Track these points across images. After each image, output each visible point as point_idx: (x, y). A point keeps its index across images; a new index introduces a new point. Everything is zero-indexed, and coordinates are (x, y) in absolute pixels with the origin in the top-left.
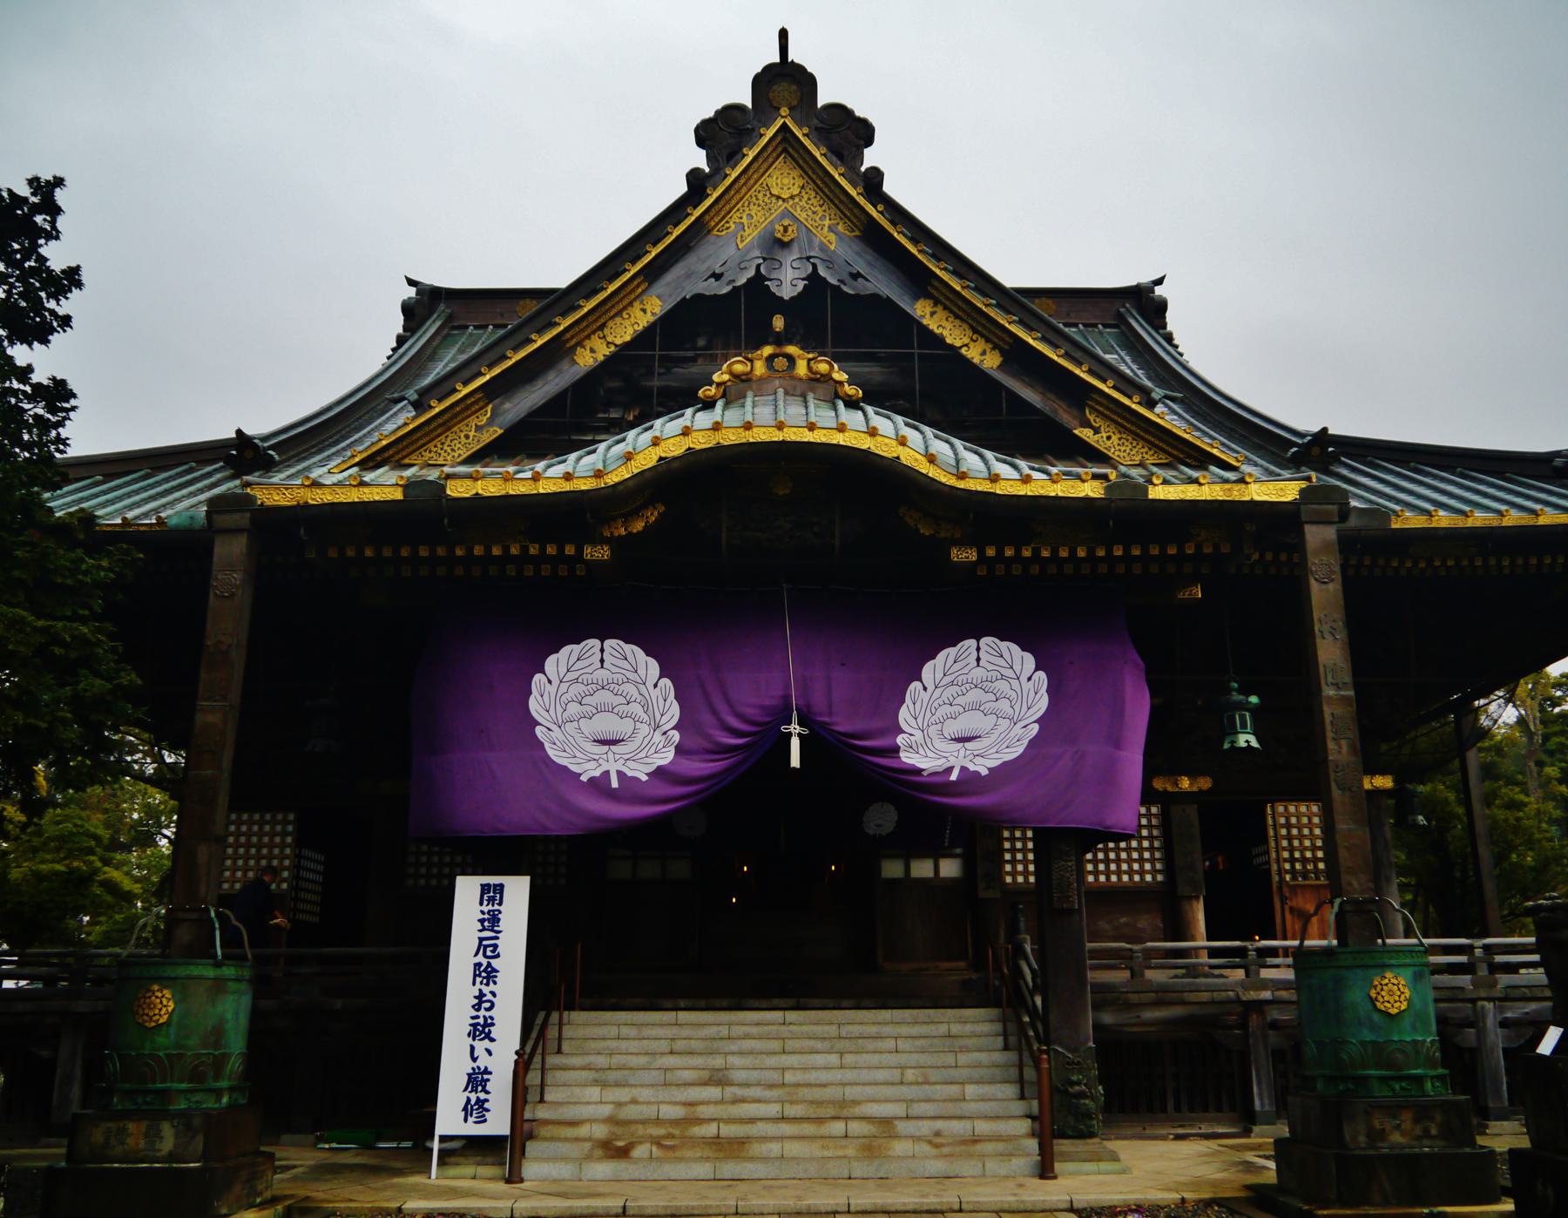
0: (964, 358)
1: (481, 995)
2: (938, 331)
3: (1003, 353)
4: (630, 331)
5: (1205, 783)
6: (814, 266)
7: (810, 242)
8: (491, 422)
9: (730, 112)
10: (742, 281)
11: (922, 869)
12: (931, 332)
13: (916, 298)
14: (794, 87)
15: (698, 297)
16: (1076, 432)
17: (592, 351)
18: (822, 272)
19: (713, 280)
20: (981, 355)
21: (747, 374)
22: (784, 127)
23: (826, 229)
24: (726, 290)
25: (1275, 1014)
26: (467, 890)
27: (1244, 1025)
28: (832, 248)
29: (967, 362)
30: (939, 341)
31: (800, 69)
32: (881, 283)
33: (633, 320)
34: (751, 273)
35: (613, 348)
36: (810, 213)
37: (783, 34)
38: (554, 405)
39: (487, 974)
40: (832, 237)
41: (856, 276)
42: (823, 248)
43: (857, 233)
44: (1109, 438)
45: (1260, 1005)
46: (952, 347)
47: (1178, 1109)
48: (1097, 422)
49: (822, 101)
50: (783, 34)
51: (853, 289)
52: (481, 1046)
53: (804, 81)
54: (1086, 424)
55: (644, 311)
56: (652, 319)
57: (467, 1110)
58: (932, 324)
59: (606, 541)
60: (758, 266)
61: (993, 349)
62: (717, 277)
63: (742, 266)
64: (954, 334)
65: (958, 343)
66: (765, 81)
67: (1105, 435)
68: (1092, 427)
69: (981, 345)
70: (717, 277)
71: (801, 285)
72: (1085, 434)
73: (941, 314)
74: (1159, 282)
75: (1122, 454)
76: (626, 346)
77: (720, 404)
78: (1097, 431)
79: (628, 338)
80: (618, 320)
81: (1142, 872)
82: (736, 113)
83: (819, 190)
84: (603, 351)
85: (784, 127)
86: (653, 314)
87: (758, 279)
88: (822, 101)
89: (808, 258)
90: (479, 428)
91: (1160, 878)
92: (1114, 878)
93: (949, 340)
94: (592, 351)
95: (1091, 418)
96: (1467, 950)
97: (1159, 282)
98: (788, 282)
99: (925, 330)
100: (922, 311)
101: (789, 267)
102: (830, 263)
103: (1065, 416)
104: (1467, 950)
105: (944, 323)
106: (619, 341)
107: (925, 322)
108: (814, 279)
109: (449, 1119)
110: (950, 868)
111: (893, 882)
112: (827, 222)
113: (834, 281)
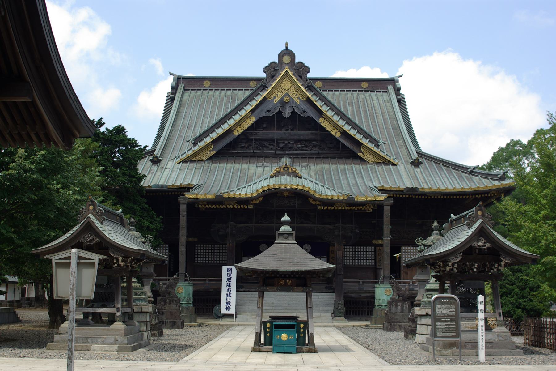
0: (331, 134)
1: (228, 289)
2: (324, 127)
3: (341, 133)
4: (247, 126)
6: (294, 109)
7: (293, 103)
8: (213, 150)
9: (272, 64)
10: (275, 113)
12: (323, 127)
14: (289, 57)
15: (264, 117)
16: (358, 154)
17: (238, 131)
19: (268, 112)
20: (336, 134)
21: (279, 171)
22: (287, 71)
23: (297, 98)
26: (225, 269)
28: (298, 103)
29: (332, 135)
30: (324, 129)
31: (291, 51)
32: (311, 113)
33: (248, 123)
34: (278, 110)
35: (243, 131)
36: (293, 94)
37: (287, 44)
39: (229, 285)
40: (298, 100)
41: (304, 111)
42: (296, 103)
43: (305, 99)
44: (366, 156)
46: (328, 131)
47: (368, 315)
48: (364, 152)
49: (297, 61)
50: (287, 44)
51: (304, 115)
52: (229, 298)
53: (292, 55)
55: (251, 120)
56: (252, 123)
57: (227, 309)
59: (252, 204)
60: (280, 108)
61: (339, 132)
62: (269, 111)
63: (276, 108)
64: (328, 127)
65: (329, 130)
66: (281, 56)
67: (365, 155)
68: (362, 153)
69: (336, 130)
70: (269, 111)
71: (290, 114)
74: (401, 76)
75: (369, 160)
76: (246, 130)
77: (274, 177)
78: (363, 154)
79: (247, 128)
80: (244, 123)
84: (240, 131)
85: (287, 71)
86: (253, 121)
87: (279, 112)
88: (297, 61)
89: (292, 106)
90: (210, 151)
91: (373, 264)
92: (362, 264)
93: (327, 129)
94: (238, 131)
95: (362, 150)
97: (401, 76)
98: (287, 113)
99: (321, 126)
100: (321, 121)
101: (287, 109)
105: (327, 125)
106: (244, 129)
107: (321, 124)
108: (293, 112)
109: (223, 311)
112: (297, 96)
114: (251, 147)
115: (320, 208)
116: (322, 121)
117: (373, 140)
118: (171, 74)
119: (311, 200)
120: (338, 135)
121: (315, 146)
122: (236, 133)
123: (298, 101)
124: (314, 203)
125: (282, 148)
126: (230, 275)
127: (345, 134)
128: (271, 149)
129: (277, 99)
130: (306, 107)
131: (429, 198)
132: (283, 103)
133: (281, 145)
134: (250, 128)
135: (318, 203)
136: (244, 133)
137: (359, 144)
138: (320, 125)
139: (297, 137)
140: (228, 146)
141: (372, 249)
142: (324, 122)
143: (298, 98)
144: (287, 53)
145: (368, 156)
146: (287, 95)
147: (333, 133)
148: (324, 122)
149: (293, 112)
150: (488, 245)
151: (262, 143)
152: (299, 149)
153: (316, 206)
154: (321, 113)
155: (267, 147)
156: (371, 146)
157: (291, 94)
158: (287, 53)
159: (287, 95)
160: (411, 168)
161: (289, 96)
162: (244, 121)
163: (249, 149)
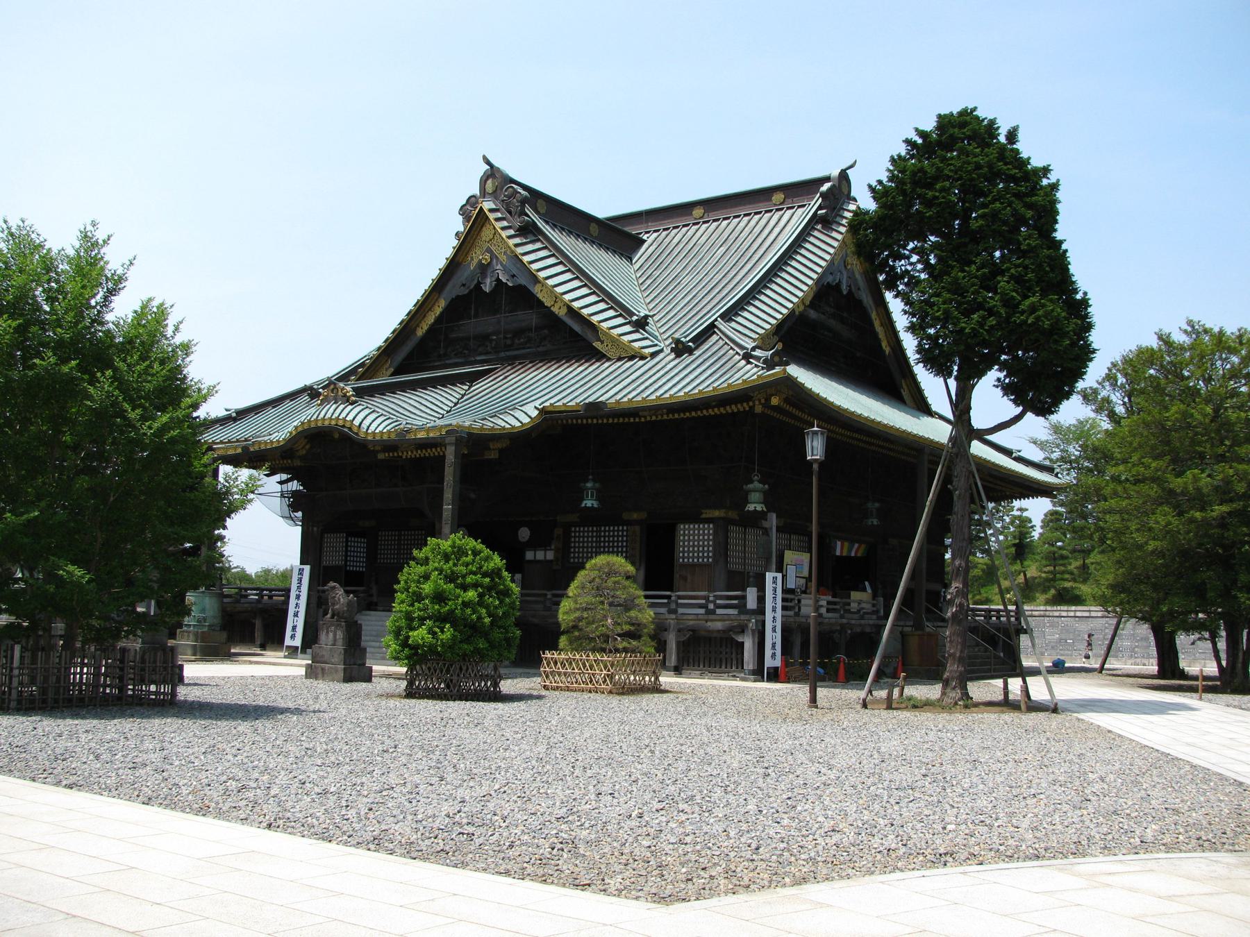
0: (553, 313)
5: (643, 515)
10: (472, 287)
11: (540, 555)
24: (467, 291)
34: (476, 282)
38: (409, 357)
39: (298, 597)
41: (513, 276)
46: (547, 307)
52: (296, 618)
62: (464, 285)
65: (549, 305)
70: (464, 285)
76: (432, 325)
81: (574, 558)
82: (473, 199)
84: (425, 328)
96: (669, 597)
98: (487, 287)
104: (669, 597)
109: (288, 642)
110: (550, 555)
111: (530, 561)
113: (504, 281)
115: (381, 456)
116: (540, 288)
122: (420, 333)
126: (301, 581)
129: (475, 261)
131: (643, 420)
132: (484, 269)
136: (431, 329)
138: (538, 298)
141: (575, 532)
142: (541, 291)
144: (493, 172)
145: (610, 346)
146: (489, 251)
148: (541, 291)
149: (498, 280)
157: (493, 248)
158: (493, 172)
162: (430, 309)
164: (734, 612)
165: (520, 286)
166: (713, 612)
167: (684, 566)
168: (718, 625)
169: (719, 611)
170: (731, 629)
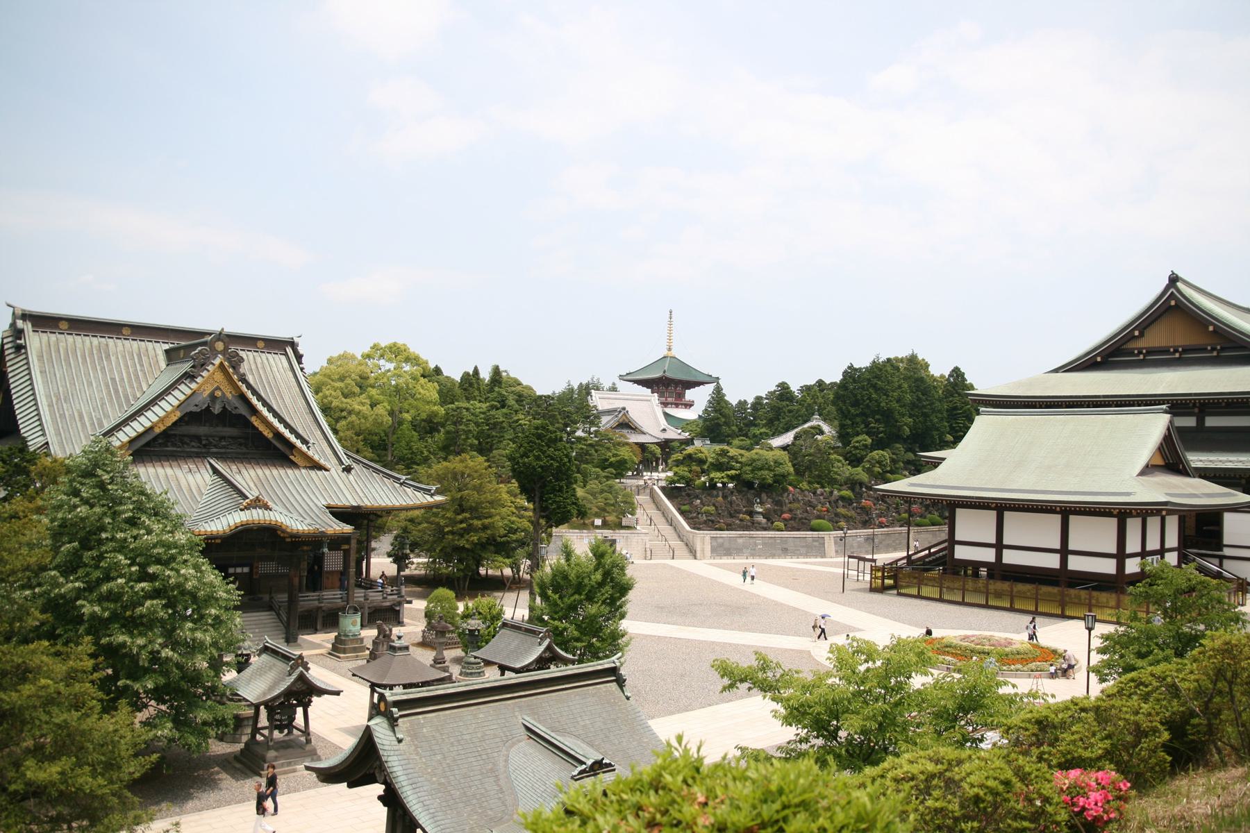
13: (252, 416)
15: (191, 412)
18: (227, 406)
20: (268, 434)
25: (324, 608)
27: (317, 611)
29: (264, 436)
30: (257, 429)
32: (243, 410)
34: (206, 405)
41: (236, 408)
42: (228, 399)
45: (321, 607)
54: (293, 455)
58: (256, 424)
62: (196, 406)
64: (261, 428)
69: (268, 431)
70: (196, 406)
72: (292, 457)
73: (258, 421)
83: (228, 380)
87: (209, 406)
98: (217, 409)
100: (253, 419)
102: (229, 403)
103: (287, 452)
108: (224, 407)
114: (169, 444)
115: (289, 540)
117: (305, 442)
118: (9, 305)
119: (279, 532)
120: (270, 436)
121: (241, 444)
123: (229, 396)
124: (282, 535)
125: (205, 446)
127: (278, 435)
128: (193, 447)
130: (238, 403)
132: (213, 397)
133: (204, 442)
134: (175, 424)
135: (286, 535)
137: (292, 446)
139: (224, 434)
140: (148, 444)
143: (231, 392)
147: (265, 433)
150: (551, 655)
151: (183, 440)
152: (224, 447)
153: (284, 538)
154: (254, 411)
155: (188, 444)
156: (304, 448)
159: (218, 388)
160: (344, 475)
161: (220, 389)
163: (167, 446)
164: (396, 597)
165: (241, 415)
166: (386, 598)
167: (327, 572)
168: (388, 604)
169: (389, 597)
170: (394, 605)
